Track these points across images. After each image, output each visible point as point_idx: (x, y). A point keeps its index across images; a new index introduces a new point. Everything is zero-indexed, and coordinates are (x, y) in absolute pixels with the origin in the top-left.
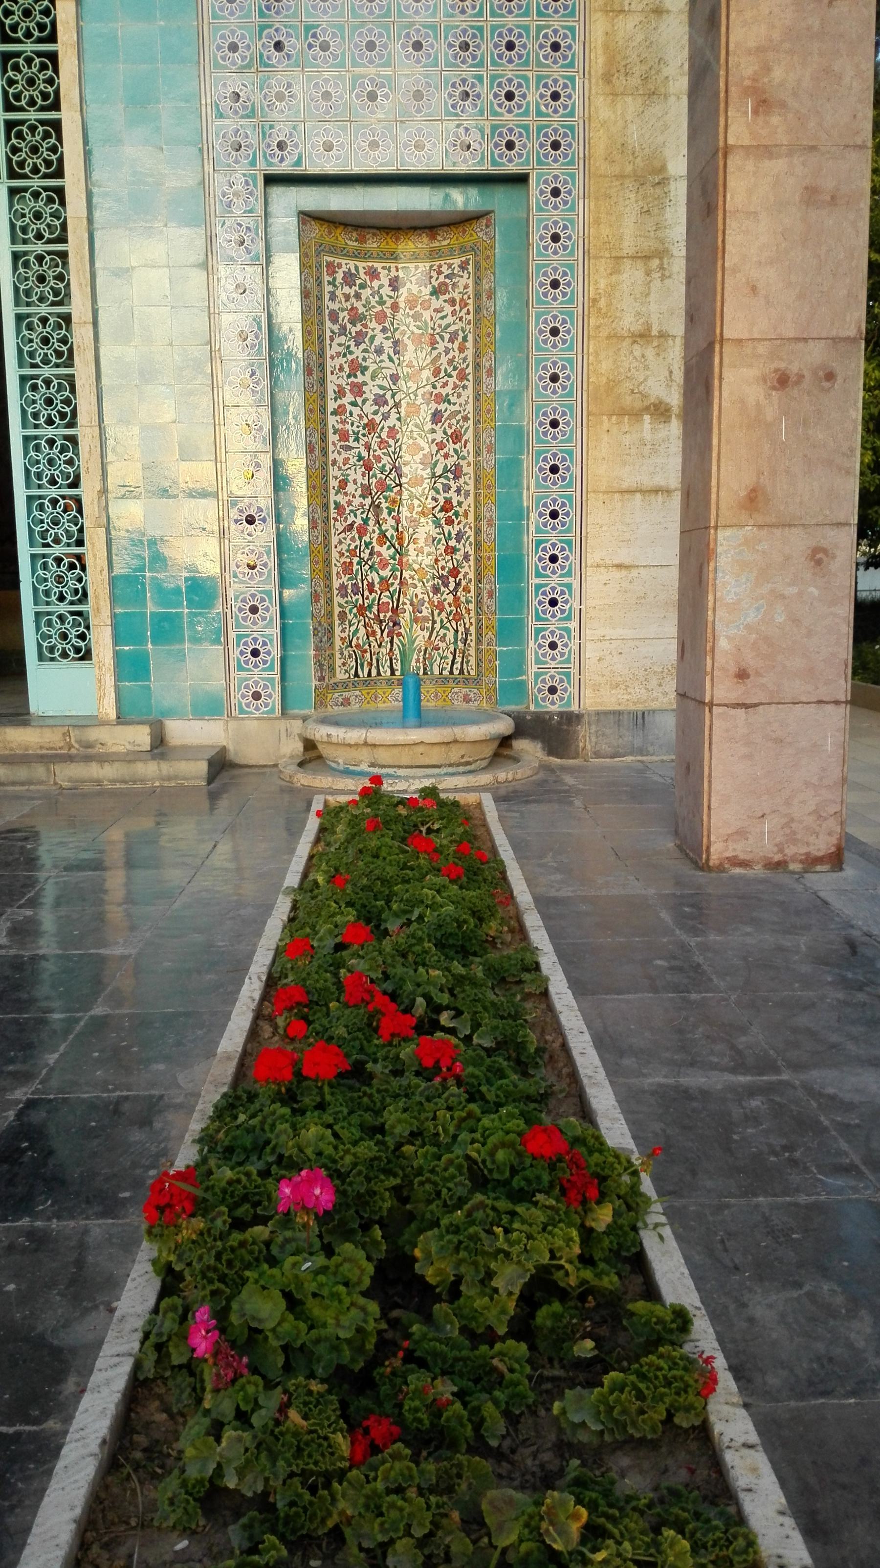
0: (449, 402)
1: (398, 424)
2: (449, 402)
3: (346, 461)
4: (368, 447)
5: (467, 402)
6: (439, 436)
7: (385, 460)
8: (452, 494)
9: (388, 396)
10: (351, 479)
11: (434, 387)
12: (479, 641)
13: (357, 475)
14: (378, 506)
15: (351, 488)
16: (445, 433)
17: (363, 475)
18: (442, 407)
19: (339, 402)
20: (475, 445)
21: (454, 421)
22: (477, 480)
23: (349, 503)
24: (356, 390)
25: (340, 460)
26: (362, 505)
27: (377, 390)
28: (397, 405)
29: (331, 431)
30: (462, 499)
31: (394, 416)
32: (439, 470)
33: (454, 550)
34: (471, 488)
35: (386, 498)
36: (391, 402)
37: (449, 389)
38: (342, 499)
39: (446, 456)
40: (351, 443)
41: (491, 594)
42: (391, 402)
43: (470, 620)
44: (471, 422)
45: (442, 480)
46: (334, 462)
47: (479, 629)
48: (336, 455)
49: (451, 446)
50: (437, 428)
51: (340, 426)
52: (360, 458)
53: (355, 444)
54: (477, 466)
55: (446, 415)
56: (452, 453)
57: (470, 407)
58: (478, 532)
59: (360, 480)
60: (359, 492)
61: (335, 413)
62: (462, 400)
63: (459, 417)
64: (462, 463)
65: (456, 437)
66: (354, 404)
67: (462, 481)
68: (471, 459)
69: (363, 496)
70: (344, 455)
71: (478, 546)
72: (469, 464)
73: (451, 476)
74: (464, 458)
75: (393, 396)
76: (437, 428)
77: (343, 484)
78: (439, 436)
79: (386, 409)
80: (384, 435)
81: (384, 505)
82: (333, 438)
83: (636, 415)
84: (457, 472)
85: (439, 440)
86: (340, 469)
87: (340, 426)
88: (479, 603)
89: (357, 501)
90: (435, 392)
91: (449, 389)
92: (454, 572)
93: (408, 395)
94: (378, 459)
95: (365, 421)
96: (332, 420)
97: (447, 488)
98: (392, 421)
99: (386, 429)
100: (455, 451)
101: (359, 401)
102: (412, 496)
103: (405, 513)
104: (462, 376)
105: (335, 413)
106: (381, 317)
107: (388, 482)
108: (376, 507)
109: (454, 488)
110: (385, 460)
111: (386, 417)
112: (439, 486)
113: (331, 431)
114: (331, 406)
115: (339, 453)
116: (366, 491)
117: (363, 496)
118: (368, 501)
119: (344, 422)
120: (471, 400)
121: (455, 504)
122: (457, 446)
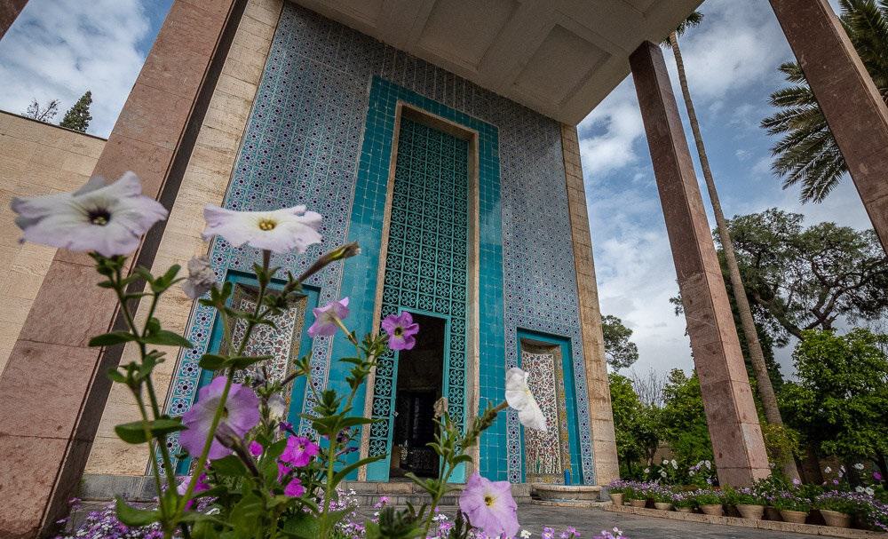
12: (562, 462)
33: (551, 433)
41: (566, 447)
43: (558, 455)
47: (562, 458)
49: (548, 403)
57: (554, 393)
58: (559, 428)
71: (560, 433)
83: (599, 399)
84: (551, 411)
88: (561, 450)
92: (551, 440)
104: (551, 384)
106: (529, 367)
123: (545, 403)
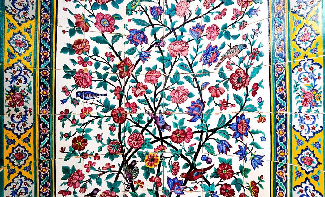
0: (228, 36)
1: (160, 65)
2: (228, 36)
3: (85, 112)
4: (119, 93)
5: (256, 32)
6: (213, 79)
7: (142, 108)
8: (232, 156)
9: (148, 31)
10: (92, 134)
11: (207, 20)
13: (102, 130)
14: (132, 166)
15: (92, 146)
16: (222, 74)
17: (112, 128)
18: (218, 42)
19: (77, 36)
20: (273, 91)
21: (235, 60)
22: (277, 145)
23: (90, 167)
24: (104, 23)
25: (76, 111)
26: (110, 167)
27: (133, 25)
28: (158, 43)
29: (60, 73)
30: (248, 165)
31: (154, 55)
32: (213, 123)
34: (265, 150)
35: (142, 156)
36: (151, 39)
37: (227, 19)
38: (76, 163)
39: (224, 105)
40: (95, 88)
42: (151, 39)
44: (264, 60)
45: (216, 136)
46: (65, 115)
48: (68, 105)
50: (211, 69)
51: (78, 67)
52: (107, 107)
53: (101, 90)
54: (279, 124)
55: (223, 52)
56: (232, 101)
59: (106, 135)
60: (105, 150)
61: (69, 49)
62: (248, 31)
63: (244, 53)
64: (247, 115)
65: (240, 80)
66: (101, 40)
67: (248, 140)
68: (266, 110)
69: (111, 155)
70: (82, 104)
72: (261, 119)
73: (231, 132)
74: (252, 109)
75: (154, 33)
76: (211, 69)
77: (79, 144)
78: (213, 79)
79: (145, 47)
80: (141, 79)
81: (140, 165)
82: (61, 81)
84: (240, 127)
85: (213, 84)
86: (74, 122)
87: (78, 67)
89: (101, 163)
90: (208, 25)
91: (227, 19)
93: (173, 30)
94: (134, 107)
95: (117, 61)
96: (63, 60)
97: (225, 148)
98: (153, 61)
99: (144, 72)
100: (237, 98)
101: (109, 36)
102: (177, 153)
103: (166, 173)
105: (69, 49)
107: (146, 136)
108: (129, 169)
109: (235, 148)
110: (142, 108)
111: (144, 57)
112: (213, 143)
113: (60, 73)
114: (63, 40)
115: (75, 102)
116: (115, 148)
117: (111, 155)
118: (119, 160)
119: (82, 62)
120: (264, 28)
121: (236, 169)
122: (241, 93)
123: (216, 92)
